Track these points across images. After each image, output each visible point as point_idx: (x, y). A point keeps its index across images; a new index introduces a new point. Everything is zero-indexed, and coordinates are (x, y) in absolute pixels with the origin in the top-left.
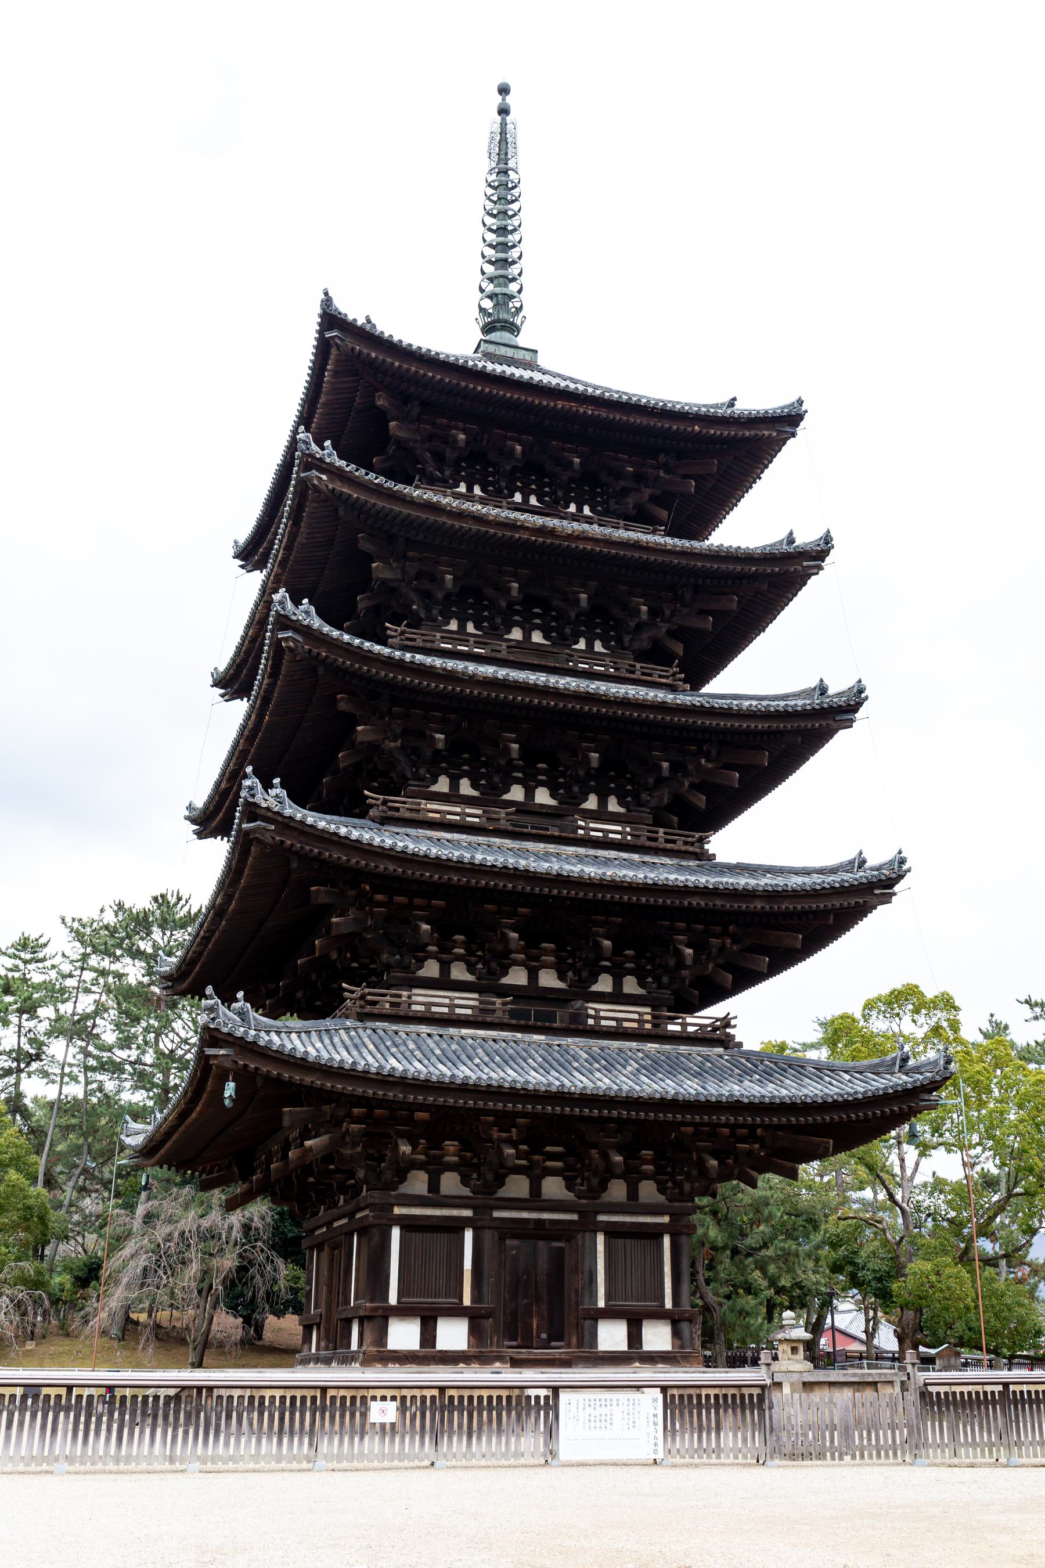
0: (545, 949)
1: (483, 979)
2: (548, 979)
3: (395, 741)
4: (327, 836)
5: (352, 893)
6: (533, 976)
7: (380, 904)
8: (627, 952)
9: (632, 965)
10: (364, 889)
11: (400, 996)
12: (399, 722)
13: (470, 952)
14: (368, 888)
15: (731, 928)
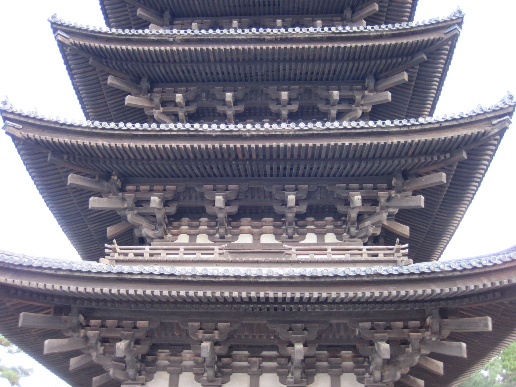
0: (265, 221)
1: (217, 242)
2: (268, 239)
3: (159, 109)
4: (52, 125)
5: (106, 184)
6: (257, 237)
7: (131, 191)
8: (327, 219)
9: (332, 227)
10: (114, 180)
11: (144, 249)
12: (157, 95)
13: (210, 227)
14: (116, 178)
15: (394, 181)
